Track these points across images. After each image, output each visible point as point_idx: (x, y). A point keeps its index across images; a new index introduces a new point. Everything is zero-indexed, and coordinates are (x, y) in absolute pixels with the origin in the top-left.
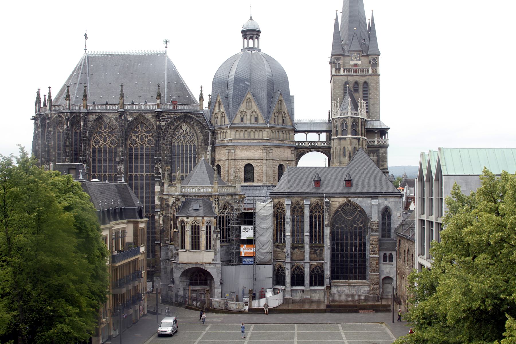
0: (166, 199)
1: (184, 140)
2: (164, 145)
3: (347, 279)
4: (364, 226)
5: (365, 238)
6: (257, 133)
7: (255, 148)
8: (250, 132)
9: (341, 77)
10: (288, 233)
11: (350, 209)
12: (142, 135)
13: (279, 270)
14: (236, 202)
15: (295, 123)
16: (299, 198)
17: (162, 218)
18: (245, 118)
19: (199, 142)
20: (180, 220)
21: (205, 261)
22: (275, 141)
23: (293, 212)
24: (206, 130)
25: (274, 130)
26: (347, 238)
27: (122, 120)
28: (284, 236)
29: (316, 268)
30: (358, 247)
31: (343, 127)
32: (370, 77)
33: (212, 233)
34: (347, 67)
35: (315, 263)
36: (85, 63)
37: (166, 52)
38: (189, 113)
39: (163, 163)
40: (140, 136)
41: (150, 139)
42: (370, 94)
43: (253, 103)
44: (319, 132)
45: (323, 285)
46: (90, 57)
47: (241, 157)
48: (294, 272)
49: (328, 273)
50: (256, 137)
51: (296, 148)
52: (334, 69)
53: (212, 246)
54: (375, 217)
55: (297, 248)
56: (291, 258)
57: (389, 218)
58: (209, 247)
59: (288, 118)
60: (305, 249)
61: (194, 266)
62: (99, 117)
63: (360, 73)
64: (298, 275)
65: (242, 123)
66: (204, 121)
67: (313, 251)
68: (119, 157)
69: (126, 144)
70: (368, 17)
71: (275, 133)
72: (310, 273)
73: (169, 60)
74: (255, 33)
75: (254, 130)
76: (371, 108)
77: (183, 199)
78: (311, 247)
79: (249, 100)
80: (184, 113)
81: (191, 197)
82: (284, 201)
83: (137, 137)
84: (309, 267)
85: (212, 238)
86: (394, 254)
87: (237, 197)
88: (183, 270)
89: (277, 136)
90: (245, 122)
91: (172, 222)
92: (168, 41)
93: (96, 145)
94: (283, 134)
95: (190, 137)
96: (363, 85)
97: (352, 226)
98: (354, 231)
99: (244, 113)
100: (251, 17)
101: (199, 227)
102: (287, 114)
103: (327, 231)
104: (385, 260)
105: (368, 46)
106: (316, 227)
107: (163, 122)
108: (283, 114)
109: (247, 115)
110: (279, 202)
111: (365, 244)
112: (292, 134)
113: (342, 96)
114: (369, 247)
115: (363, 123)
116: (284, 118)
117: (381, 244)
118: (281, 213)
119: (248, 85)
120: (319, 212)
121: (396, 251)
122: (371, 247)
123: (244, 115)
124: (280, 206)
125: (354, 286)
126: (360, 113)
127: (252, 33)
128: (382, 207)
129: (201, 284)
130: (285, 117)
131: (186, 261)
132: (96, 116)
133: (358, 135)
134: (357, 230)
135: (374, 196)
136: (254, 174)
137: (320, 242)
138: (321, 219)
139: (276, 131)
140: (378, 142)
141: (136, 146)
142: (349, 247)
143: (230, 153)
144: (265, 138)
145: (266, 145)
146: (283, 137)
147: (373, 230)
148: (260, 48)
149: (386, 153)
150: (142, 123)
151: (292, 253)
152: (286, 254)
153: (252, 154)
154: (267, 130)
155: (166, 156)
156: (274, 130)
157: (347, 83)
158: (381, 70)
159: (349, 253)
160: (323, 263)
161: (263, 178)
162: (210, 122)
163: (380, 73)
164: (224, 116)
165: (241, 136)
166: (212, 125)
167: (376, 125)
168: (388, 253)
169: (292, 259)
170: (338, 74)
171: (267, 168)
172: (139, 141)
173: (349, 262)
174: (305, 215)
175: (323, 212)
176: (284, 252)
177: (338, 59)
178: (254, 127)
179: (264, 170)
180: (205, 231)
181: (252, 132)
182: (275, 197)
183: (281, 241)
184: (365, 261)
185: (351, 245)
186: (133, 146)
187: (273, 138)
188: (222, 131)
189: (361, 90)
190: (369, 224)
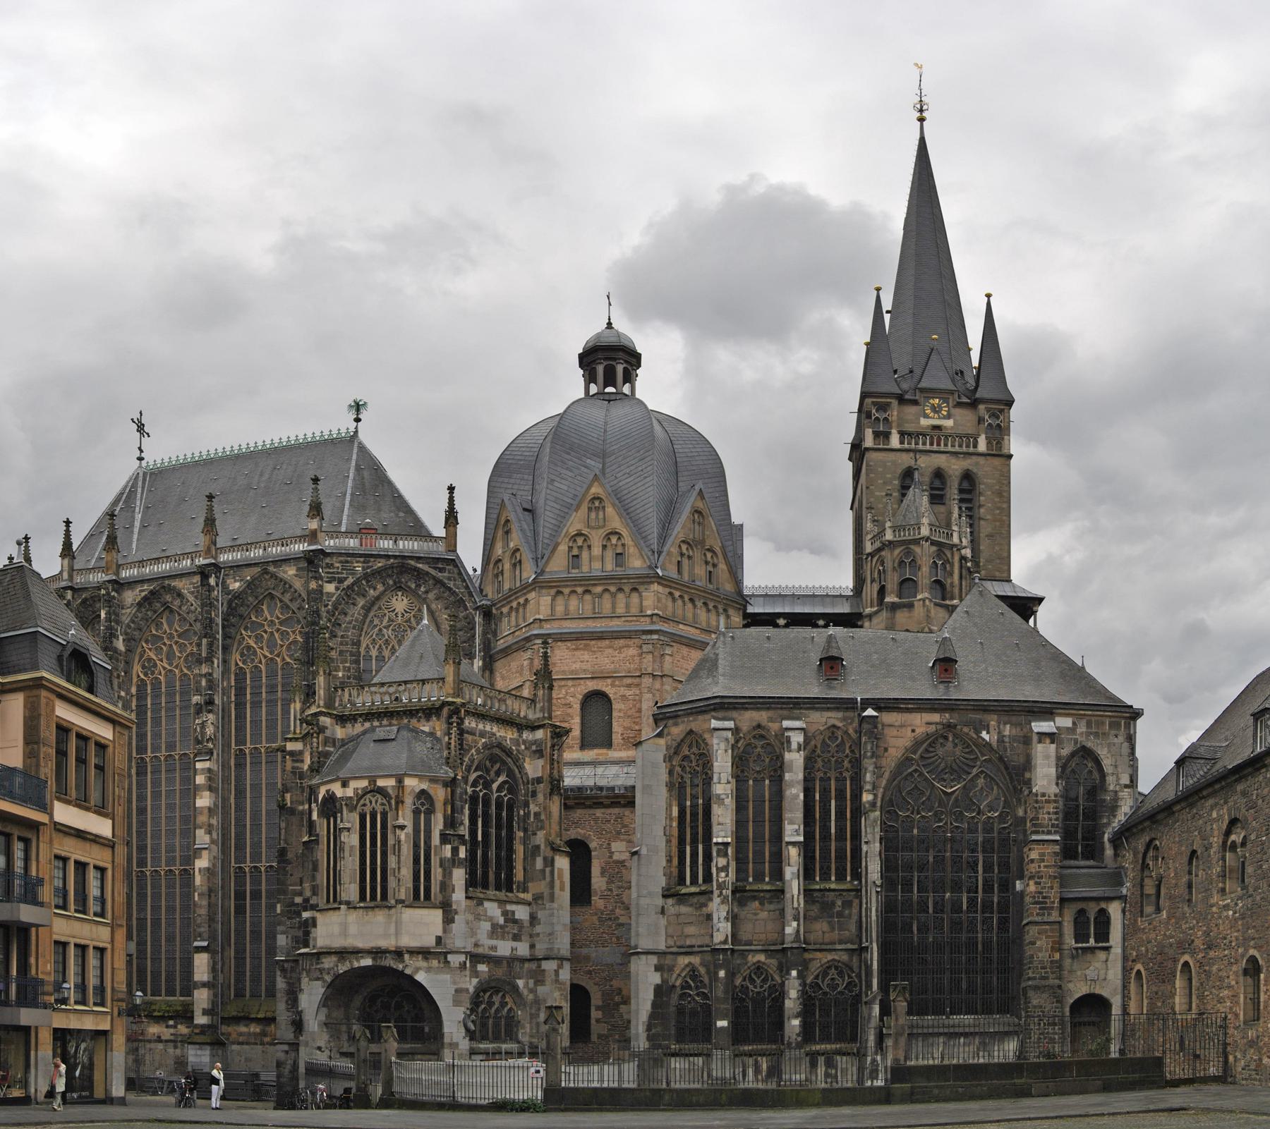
2: (333, 654)
6: (620, 596)
7: (616, 642)
8: (600, 596)
14: (535, 752)
15: (747, 596)
18: (585, 555)
21: (407, 941)
22: (681, 626)
23: (740, 762)
25: (677, 594)
33: (436, 840)
43: (610, 510)
47: (572, 672)
50: (620, 610)
53: (435, 888)
55: (754, 898)
58: (421, 896)
65: (577, 571)
68: (198, 691)
71: (680, 602)
75: (613, 589)
78: (808, 893)
79: (597, 503)
85: (435, 861)
87: (540, 734)
89: (689, 615)
90: (585, 568)
93: (146, 675)
94: (708, 611)
99: (580, 541)
101: (384, 815)
109: (589, 547)
110: (691, 732)
116: (710, 568)
120: (839, 763)
123: (580, 548)
127: (612, 355)
130: (714, 566)
136: (615, 724)
137: (841, 877)
139: (686, 598)
144: (649, 612)
145: (651, 632)
154: (655, 587)
156: (677, 594)
161: (643, 732)
164: (520, 561)
165: (572, 608)
166: (486, 596)
180: (409, 829)
181: (607, 596)
183: (694, 881)
188: (514, 604)
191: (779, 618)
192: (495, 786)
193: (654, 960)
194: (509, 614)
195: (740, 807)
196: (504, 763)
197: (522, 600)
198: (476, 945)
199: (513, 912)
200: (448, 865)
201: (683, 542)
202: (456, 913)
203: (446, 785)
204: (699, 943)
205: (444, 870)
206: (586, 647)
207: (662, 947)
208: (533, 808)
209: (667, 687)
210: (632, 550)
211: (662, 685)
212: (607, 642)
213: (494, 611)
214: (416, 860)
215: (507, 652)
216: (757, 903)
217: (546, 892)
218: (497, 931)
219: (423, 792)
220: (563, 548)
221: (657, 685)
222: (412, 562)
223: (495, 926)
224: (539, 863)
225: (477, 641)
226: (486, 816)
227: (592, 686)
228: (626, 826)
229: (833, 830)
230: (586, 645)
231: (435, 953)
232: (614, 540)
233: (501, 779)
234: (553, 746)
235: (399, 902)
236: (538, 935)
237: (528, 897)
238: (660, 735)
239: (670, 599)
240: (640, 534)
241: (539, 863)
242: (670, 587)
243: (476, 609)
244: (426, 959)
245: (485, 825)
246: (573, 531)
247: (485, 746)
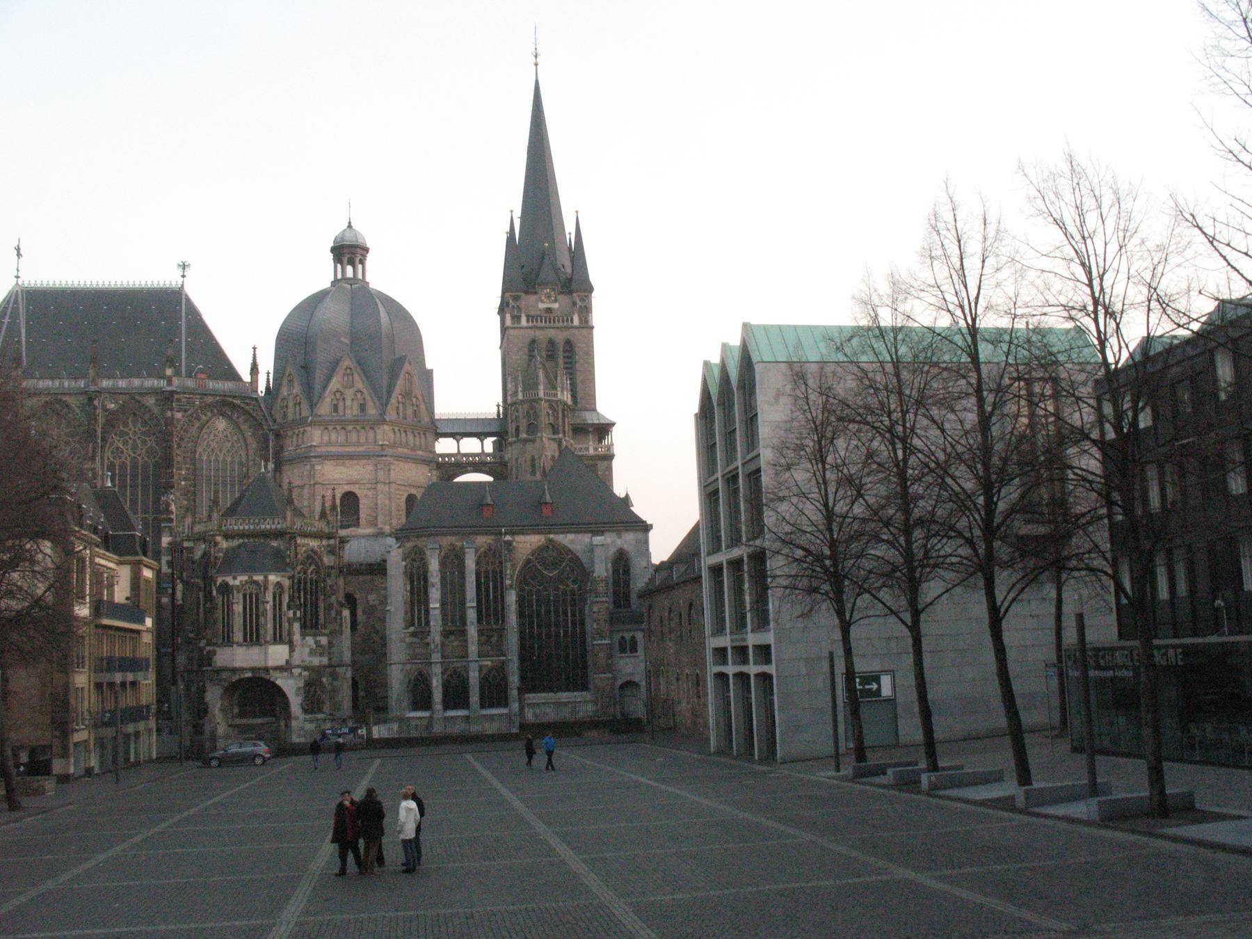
0: (187, 548)
1: (221, 451)
2: (180, 459)
3: (552, 691)
4: (580, 588)
5: (582, 611)
9: (522, 331)
10: (435, 605)
12: (134, 440)
14: (329, 551)
16: (454, 538)
17: (180, 587)
18: (341, 404)
19: (250, 454)
20: (218, 584)
21: (271, 663)
22: (400, 449)
23: (443, 564)
24: (263, 429)
25: (396, 429)
26: (548, 612)
27: (95, 408)
28: (427, 612)
29: (490, 672)
32: (576, 332)
34: (532, 313)
35: (489, 663)
36: (16, 302)
37: (182, 286)
38: (230, 396)
39: (178, 494)
40: (131, 442)
41: (151, 447)
42: (576, 362)
43: (356, 376)
44: (481, 436)
45: (506, 705)
46: (28, 292)
47: (334, 480)
48: (448, 681)
49: (514, 679)
50: (362, 440)
51: (440, 466)
52: (508, 316)
53: (285, 634)
54: (602, 570)
56: (442, 655)
57: (627, 571)
58: (278, 639)
59: (423, 407)
60: (469, 636)
61: (249, 675)
62: (47, 402)
63: (557, 324)
65: (335, 414)
66: (259, 413)
67: (483, 639)
69: (102, 458)
70: (570, 228)
71: (398, 434)
72: (480, 682)
73: (188, 301)
74: (359, 251)
76: (579, 388)
77: (224, 544)
78: (481, 633)
80: (220, 395)
81: (241, 541)
82: (424, 544)
83: (125, 443)
84: (477, 669)
85: (285, 619)
86: (639, 636)
87: (332, 542)
88: (226, 685)
89: (404, 441)
91: (201, 595)
92: (189, 265)
94: (415, 436)
95: (233, 446)
96: (564, 348)
97: (557, 589)
100: (350, 223)
102: (420, 398)
103: (512, 598)
104: (623, 650)
105: (569, 277)
106: (488, 595)
107: (178, 411)
108: (414, 400)
109: (344, 399)
111: (582, 623)
112: (430, 437)
113: (525, 366)
114: (591, 626)
115: (566, 412)
116: (415, 408)
117: (613, 619)
118: (419, 568)
119: (347, 344)
121: (642, 630)
122: (595, 626)
123: (338, 400)
124: (418, 555)
125: (566, 704)
126: (559, 393)
128: (613, 550)
129: (263, 714)
131: (229, 665)
132: (38, 401)
133: (558, 433)
135: (597, 529)
136: (361, 512)
138: (499, 577)
139: (402, 430)
140: (596, 449)
141: (124, 463)
143: (312, 473)
144: (380, 443)
146: (415, 445)
148: (367, 280)
149: (610, 469)
150: (135, 414)
151: (443, 645)
153: (356, 473)
155: (185, 479)
157: (533, 341)
158: (599, 316)
160: (503, 663)
162: (272, 416)
163: (594, 324)
164: (300, 403)
167: (590, 418)
168: (627, 636)
169: (443, 657)
170: (516, 326)
172: (127, 450)
174: (467, 568)
177: (516, 298)
178: (357, 421)
179: (379, 502)
180: (271, 603)
182: (408, 538)
184: (584, 655)
185: (557, 625)
186: (117, 462)
187: (395, 443)
189: (561, 354)
190: (589, 584)
192: (309, 572)
193: (400, 667)
194: (292, 437)
195: (443, 586)
196: (313, 559)
197: (301, 430)
198: (303, 661)
199: (320, 641)
200: (290, 622)
201: (400, 394)
202: (296, 646)
203: (289, 578)
205: (289, 624)
206: (343, 464)
208: (329, 582)
209: (392, 490)
210: (370, 404)
212: (355, 461)
213: (282, 432)
214: (274, 619)
215: (291, 461)
217: (337, 628)
218: (312, 652)
219: (278, 583)
220: (328, 400)
222: (230, 399)
223: (311, 649)
224: (333, 613)
225: (271, 451)
226: (305, 589)
227: (347, 488)
230: (343, 463)
231: (286, 668)
232: (359, 395)
233: (313, 567)
234: (339, 548)
235: (266, 642)
236: (333, 653)
237: (327, 631)
238: (399, 547)
240: (375, 389)
241: (333, 613)
243: (270, 430)
244: (281, 672)
245: (305, 593)
246: (334, 390)
247: (305, 552)
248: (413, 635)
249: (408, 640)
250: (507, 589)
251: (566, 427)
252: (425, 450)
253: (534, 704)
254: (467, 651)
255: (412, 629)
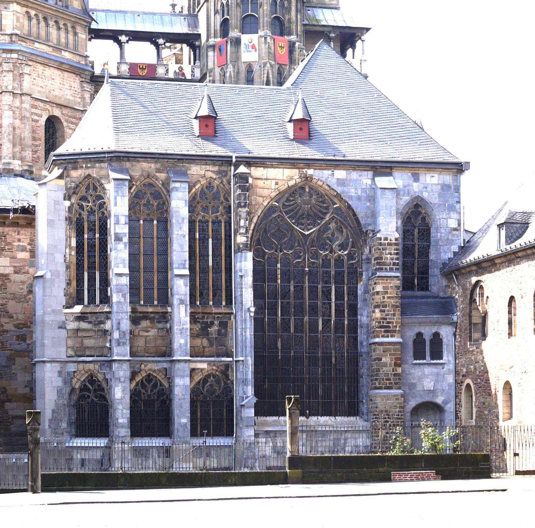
4: (350, 256)
11: (309, 203)
13: (89, 390)
22: (37, 45)
25: (33, 13)
26: (299, 290)
28: (105, 282)
29: (205, 380)
30: (333, 318)
31: (245, 10)
35: (204, 366)
60: (176, 319)
64: (149, 403)
67: (197, 327)
71: (34, 21)
84: (188, 372)
89: (43, 33)
94: (59, 29)
98: (321, 270)
111: (354, 310)
118: (91, 212)
122: (378, 314)
134: (329, 266)
142: (306, 318)
144: (9, 32)
145: (11, 51)
146: (59, 40)
147: (384, 264)
152: (116, 335)
156: (33, 13)
159: (306, 336)
160: (228, 366)
171: (15, 118)
173: (306, 362)
175: (228, 209)
176: (105, 332)
183: (92, 300)
190: (367, 250)
191: (121, 35)
204: (98, 354)
207: (64, 357)
211: (22, 102)
216: (148, 321)
221: (17, 103)
228: (10, 244)
229: (211, 264)
239: (26, 16)
242: (27, 6)
248: (81, 317)
249: (72, 325)
250: (239, 250)
251: (299, 28)
252: (75, 51)
253: (275, 432)
254: (171, 343)
255: (78, 309)
